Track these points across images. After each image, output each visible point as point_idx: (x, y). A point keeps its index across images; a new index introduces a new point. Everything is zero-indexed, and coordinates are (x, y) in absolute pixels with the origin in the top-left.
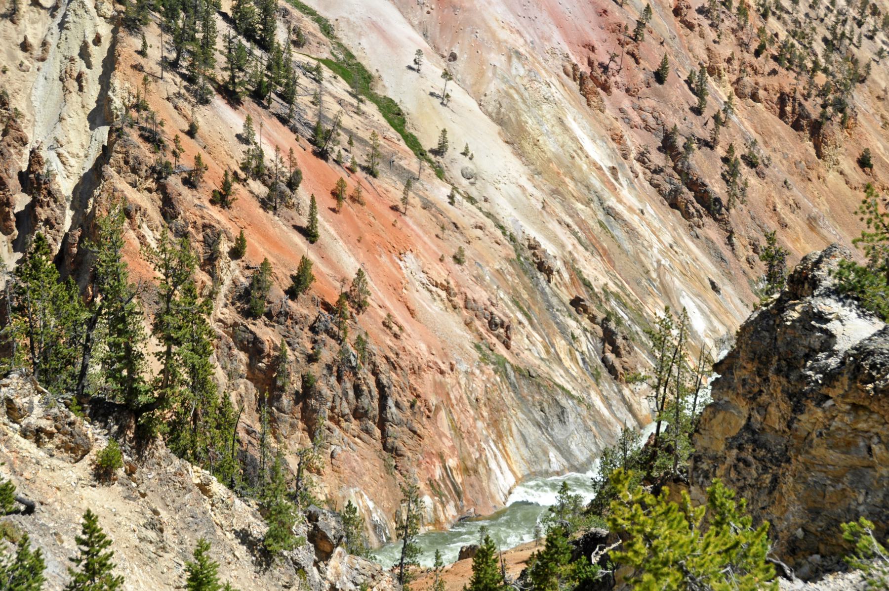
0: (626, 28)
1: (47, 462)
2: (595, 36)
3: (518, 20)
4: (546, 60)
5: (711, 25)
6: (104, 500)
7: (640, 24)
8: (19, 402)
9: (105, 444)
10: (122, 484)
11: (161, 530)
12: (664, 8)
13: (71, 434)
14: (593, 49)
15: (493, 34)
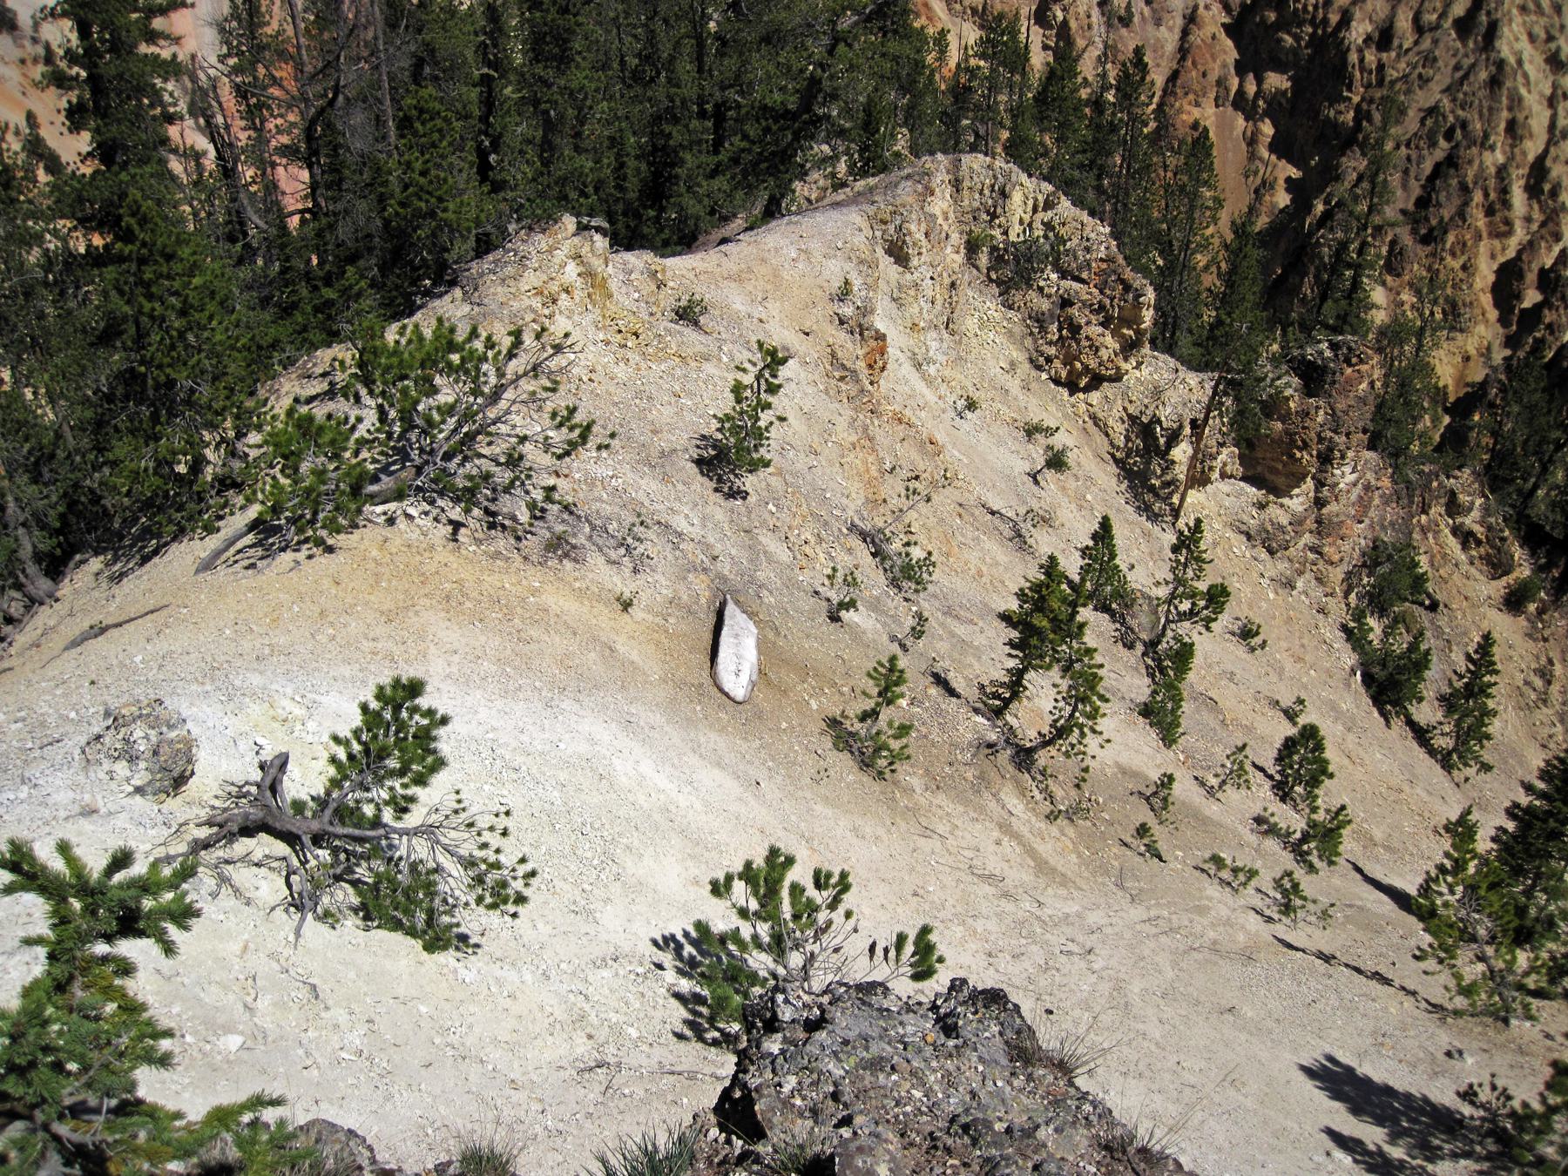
1: (1465, 567)
6: (1507, 629)
8: (1463, 498)
9: (1527, 573)
10: (1528, 620)
11: (1549, 683)
13: (1499, 550)
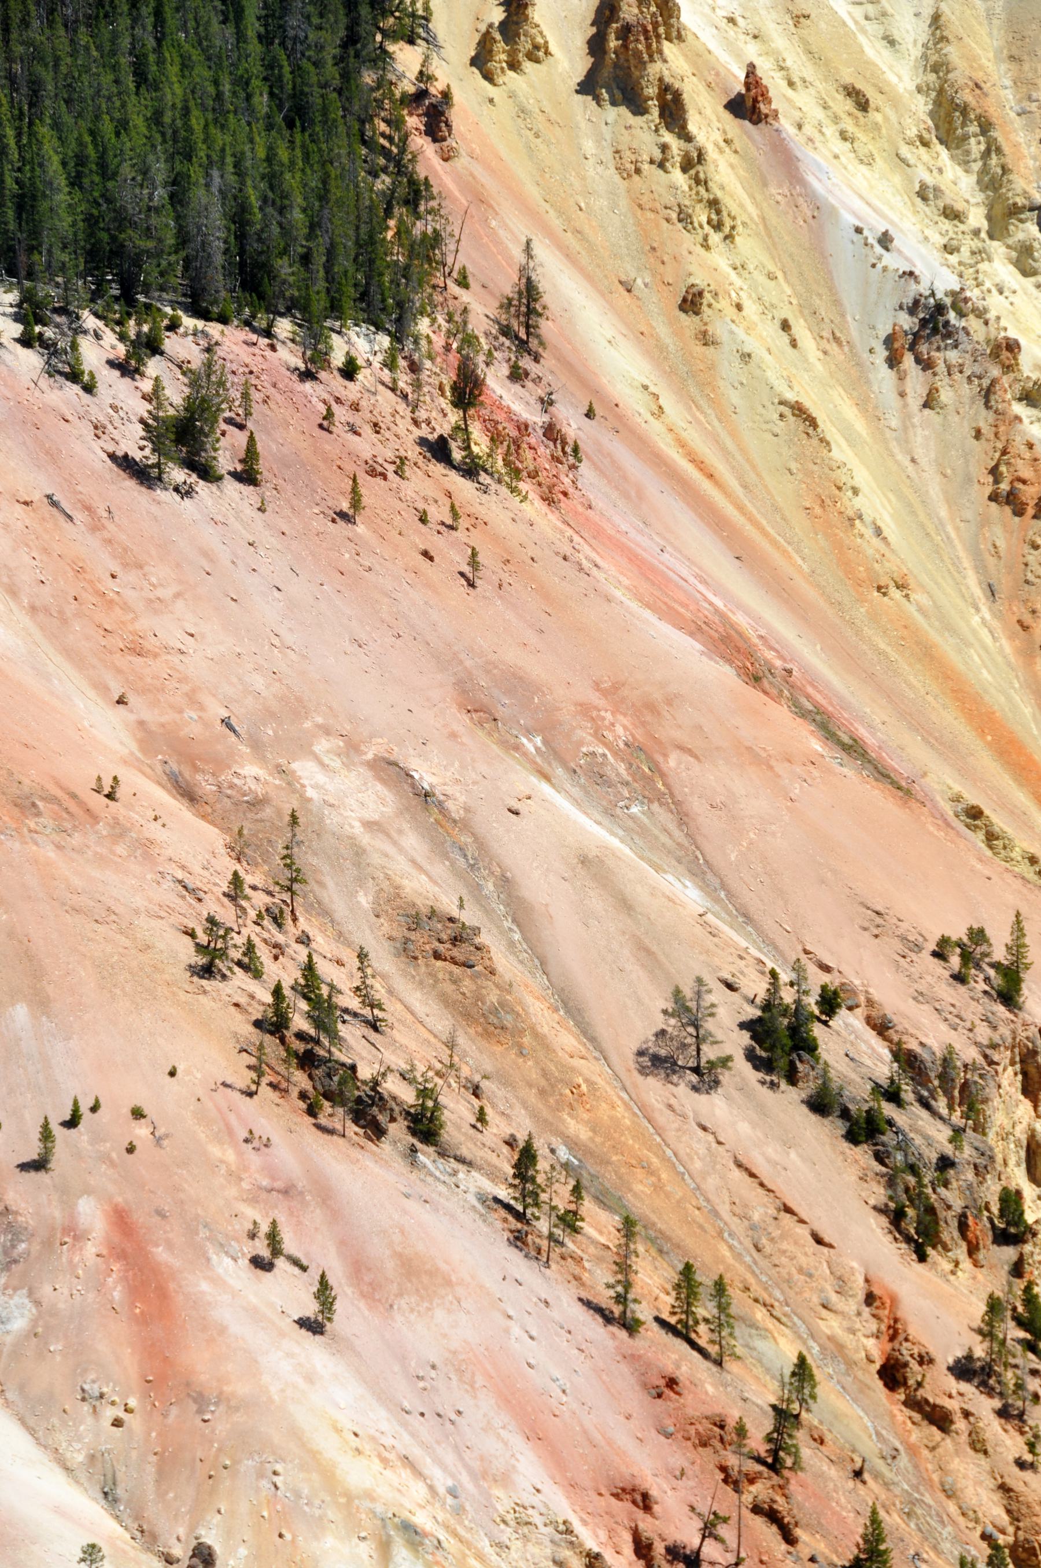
0: (741, 1431)
2: (648, 1462)
3: (405, 1425)
4: (501, 1547)
5: (1003, 1413)
7: (784, 1418)
12: (850, 1364)
14: (645, 1503)
15: (329, 1477)
